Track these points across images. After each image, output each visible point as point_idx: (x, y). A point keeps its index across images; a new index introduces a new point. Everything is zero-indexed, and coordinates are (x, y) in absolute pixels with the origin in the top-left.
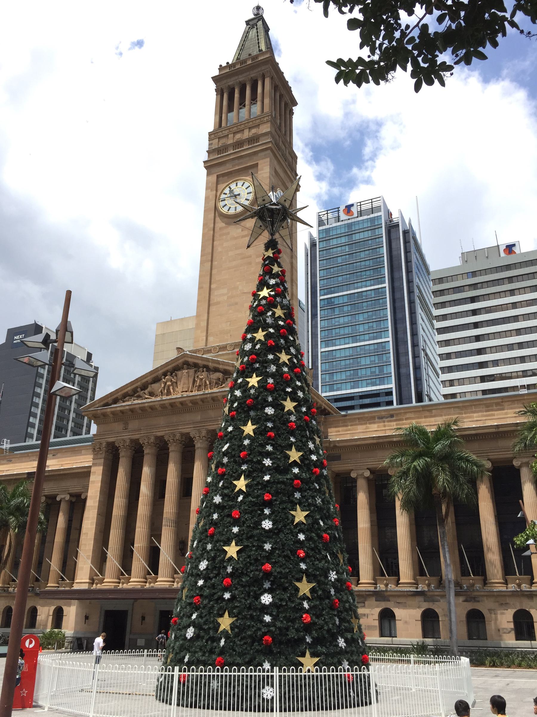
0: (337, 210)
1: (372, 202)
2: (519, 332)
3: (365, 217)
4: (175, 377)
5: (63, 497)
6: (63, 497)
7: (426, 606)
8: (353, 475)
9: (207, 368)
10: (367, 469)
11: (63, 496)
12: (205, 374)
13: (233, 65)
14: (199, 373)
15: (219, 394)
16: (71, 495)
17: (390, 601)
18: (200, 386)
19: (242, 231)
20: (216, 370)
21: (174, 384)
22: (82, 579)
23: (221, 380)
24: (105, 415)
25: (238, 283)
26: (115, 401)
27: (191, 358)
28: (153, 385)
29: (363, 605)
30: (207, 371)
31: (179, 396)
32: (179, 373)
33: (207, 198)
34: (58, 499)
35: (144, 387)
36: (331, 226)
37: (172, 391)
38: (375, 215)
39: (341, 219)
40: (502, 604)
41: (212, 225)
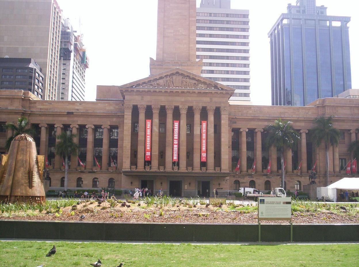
2: (228, 51)
4: (171, 79)
5: (90, 127)
6: (90, 127)
7: (266, 179)
8: (241, 130)
10: (247, 128)
11: (90, 126)
12: (188, 80)
14: (184, 79)
17: (253, 178)
20: (194, 79)
22: (126, 167)
23: (196, 84)
25: (180, 29)
29: (243, 179)
32: (174, 77)
40: (292, 179)
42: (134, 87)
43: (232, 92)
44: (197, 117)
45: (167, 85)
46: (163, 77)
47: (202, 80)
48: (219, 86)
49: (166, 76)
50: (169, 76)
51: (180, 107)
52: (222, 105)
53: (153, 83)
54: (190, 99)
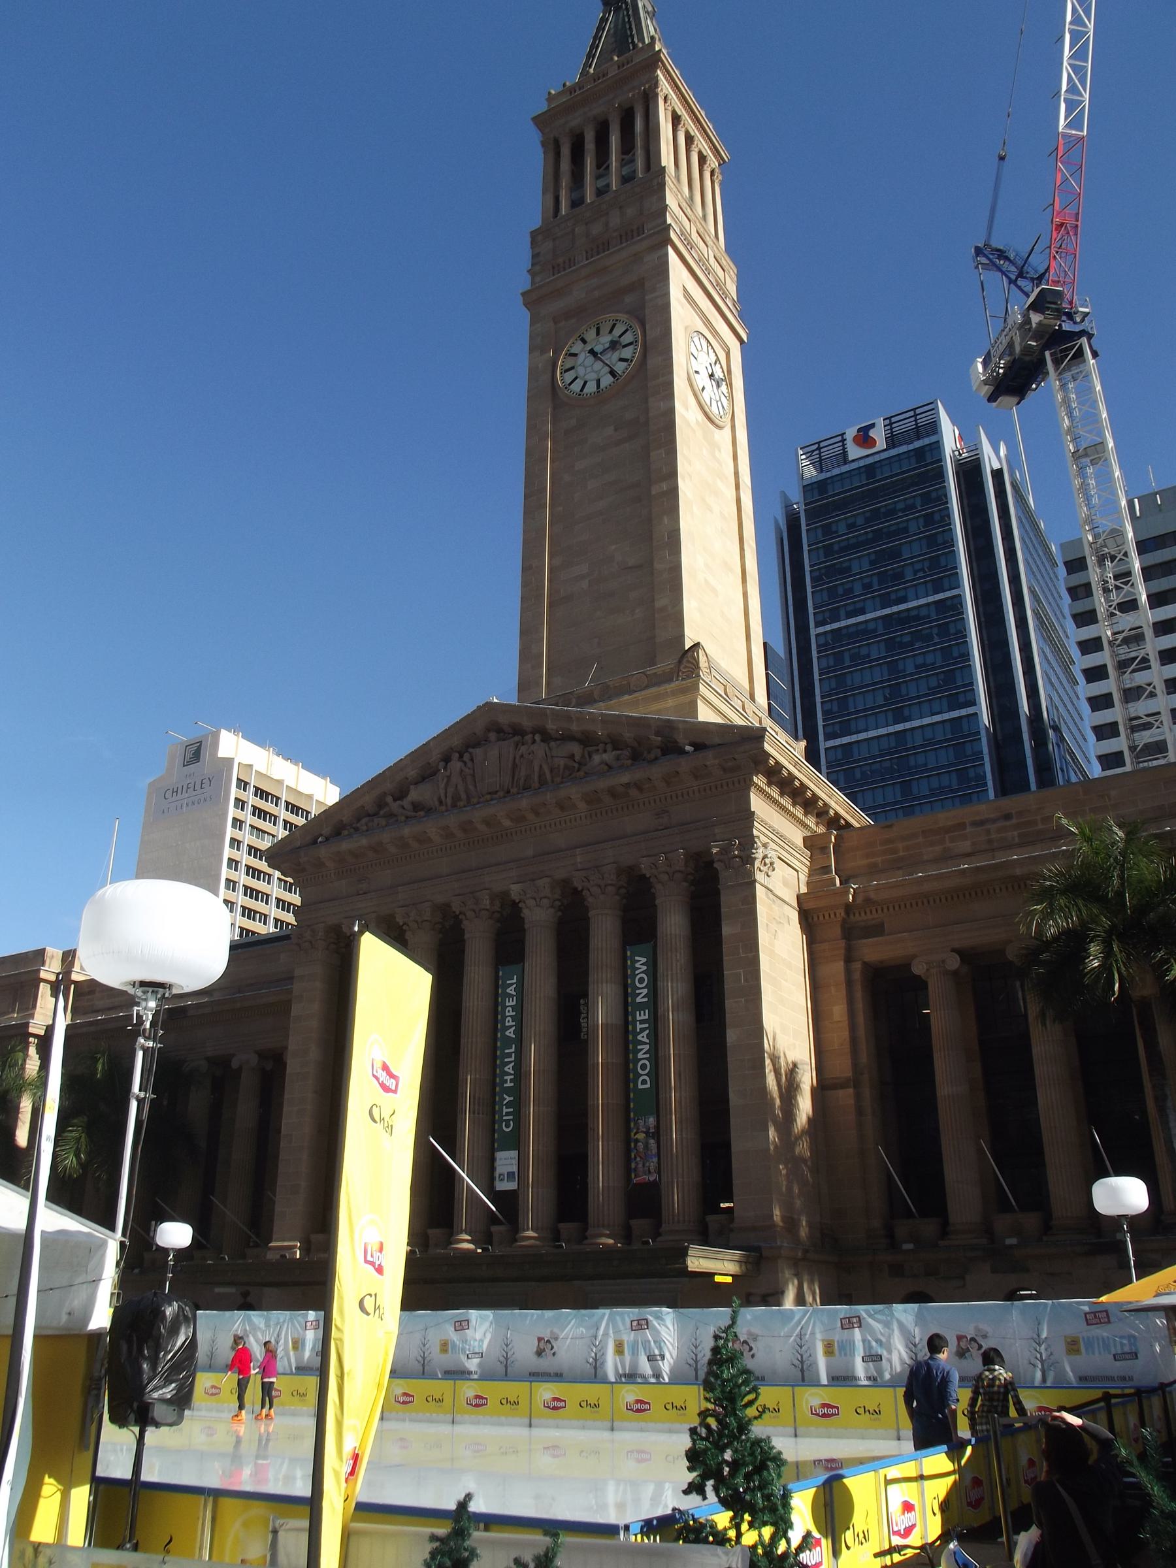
0: (840, 438)
1: (915, 415)
3: (903, 449)
9: (546, 737)
10: (953, 950)
12: (540, 749)
13: (579, 85)
16: (262, 1055)
19: (616, 430)
23: (577, 758)
30: (543, 741)
33: (533, 374)
34: (235, 1064)
35: (400, 795)
36: (829, 475)
38: (927, 441)
39: (851, 458)
44: (604, 932)
48: (680, 738)
53: (394, 806)
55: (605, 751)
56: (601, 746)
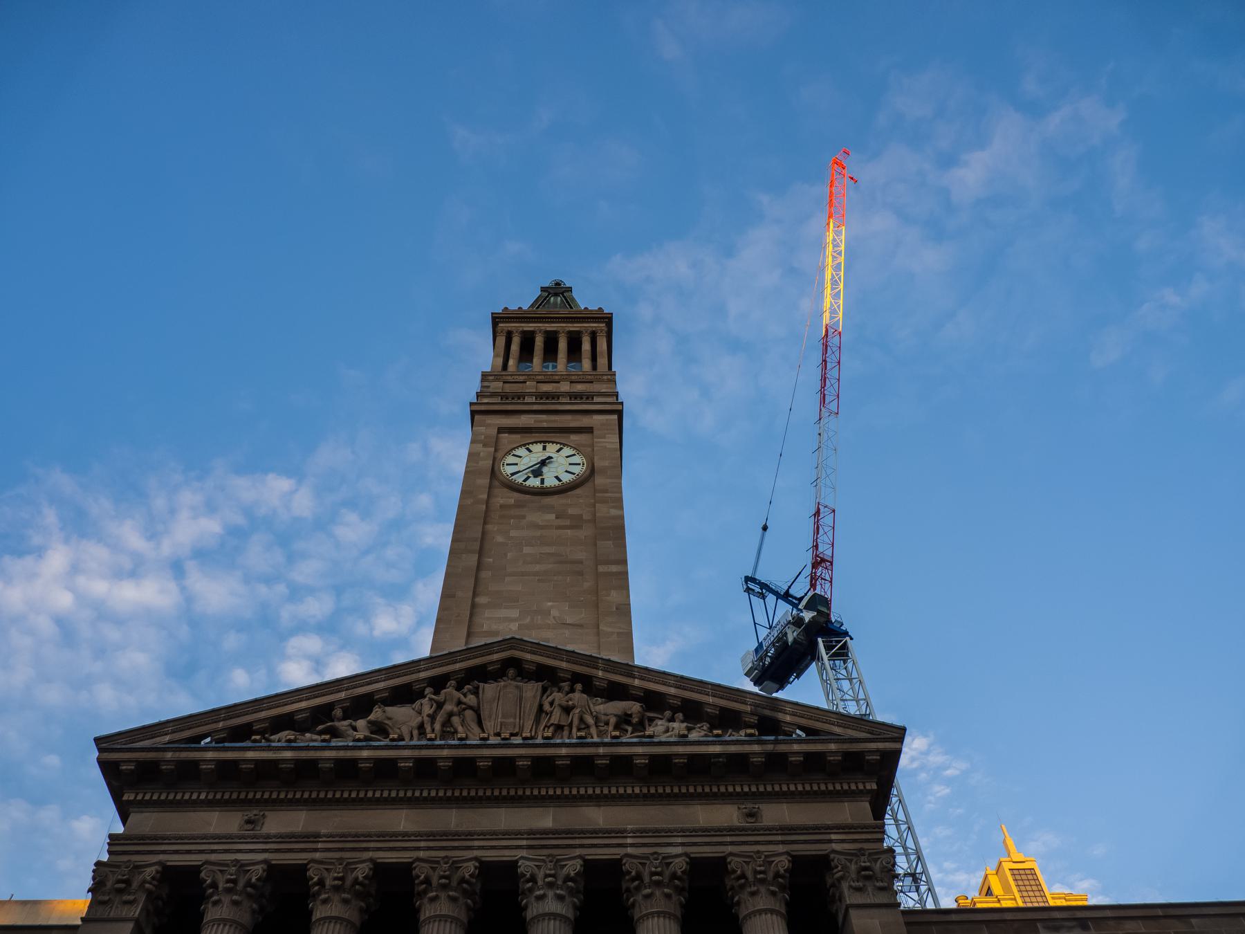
9: (588, 685)
12: (578, 697)
14: (558, 696)
15: (640, 750)
18: (559, 728)
20: (615, 692)
21: (469, 713)
23: (635, 720)
24: (188, 773)
26: (241, 733)
27: (534, 653)
28: (388, 709)
30: (583, 692)
31: (493, 740)
32: (489, 690)
37: (460, 729)
41: (485, 496)
42: (208, 740)
43: (881, 745)
45: (437, 726)
46: (416, 687)
47: (672, 691)
48: (788, 718)
49: (438, 683)
50: (459, 688)
51: (525, 867)
52: (838, 845)
54: (597, 816)
55: (672, 720)
56: (668, 713)
